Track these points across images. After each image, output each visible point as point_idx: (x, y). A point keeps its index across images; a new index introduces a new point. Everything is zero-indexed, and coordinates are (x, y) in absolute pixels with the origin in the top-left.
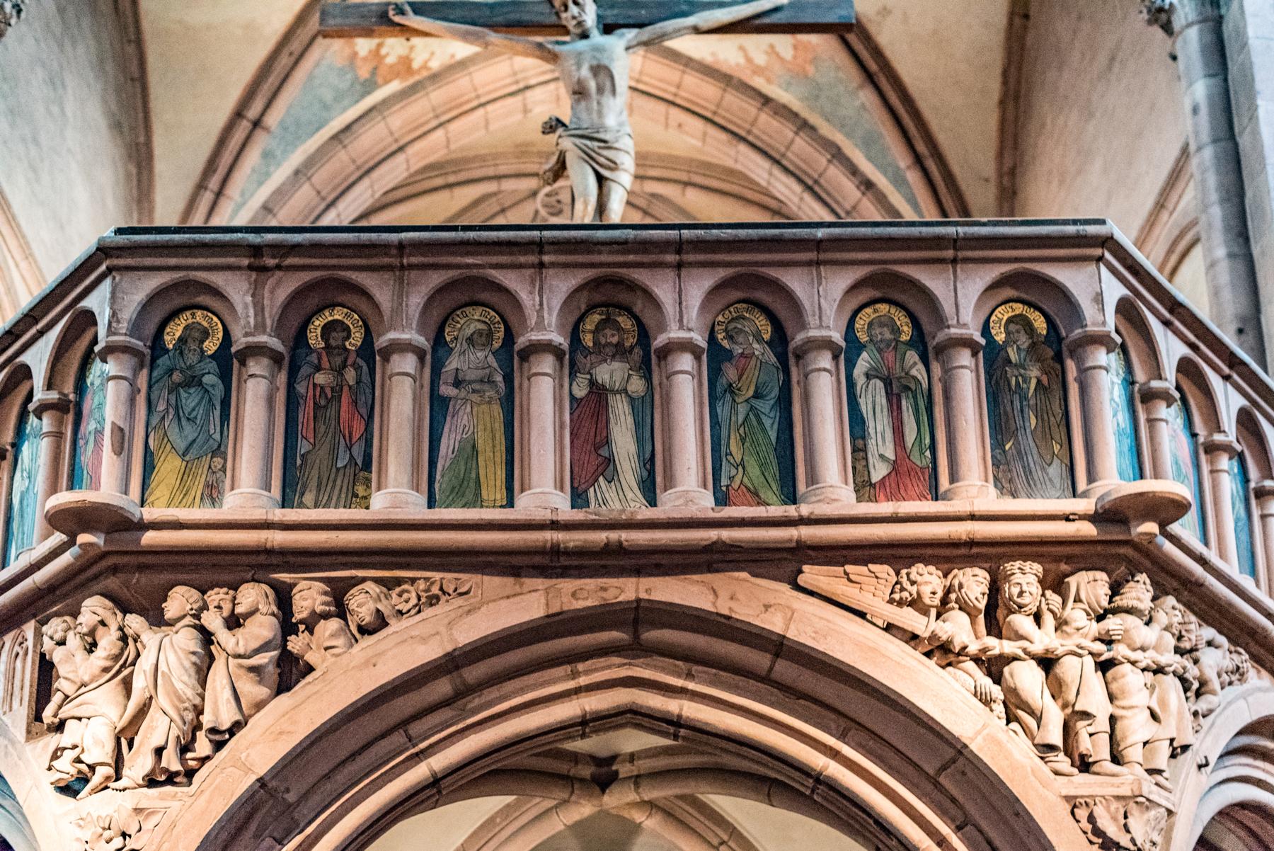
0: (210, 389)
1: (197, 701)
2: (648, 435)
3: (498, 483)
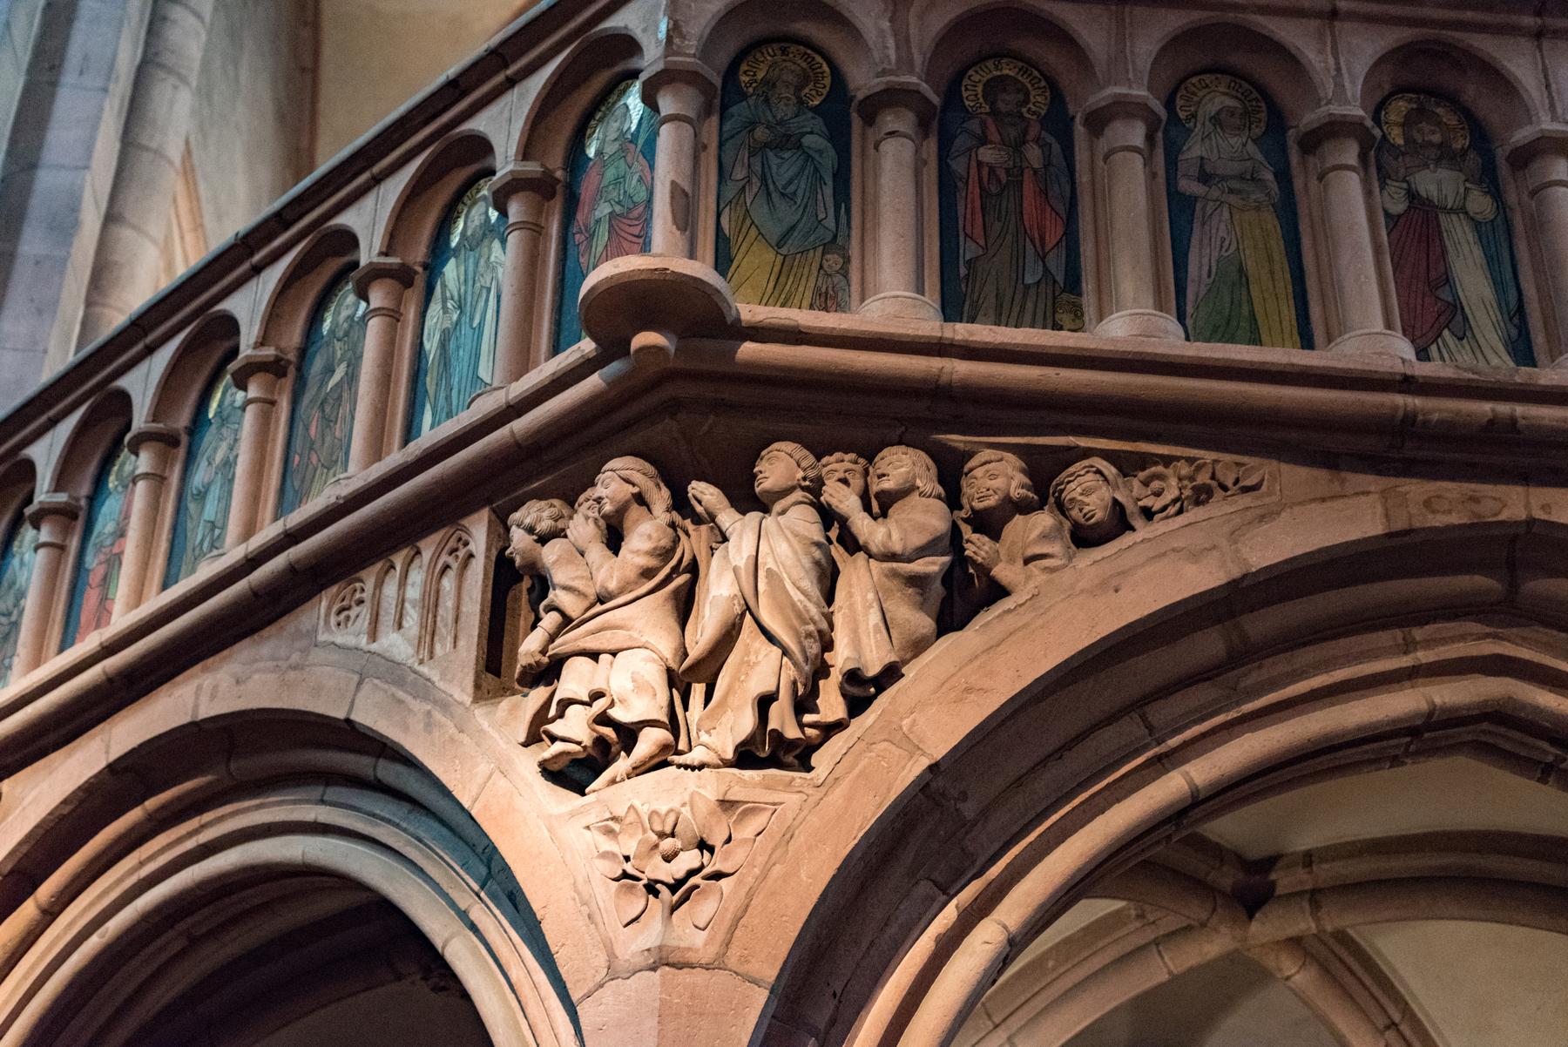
0: (817, 156)
1: (824, 626)
2: (1508, 275)
3: (1286, 324)
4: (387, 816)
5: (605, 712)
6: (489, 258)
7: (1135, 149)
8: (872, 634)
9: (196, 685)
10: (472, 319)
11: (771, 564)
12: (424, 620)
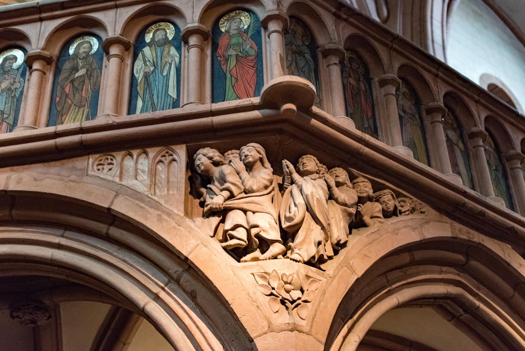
5: (258, 233)
6: (169, 52)
7: (393, 95)
8: (342, 229)
9: (6, 175)
10: (162, 72)
11: (318, 197)
12: (152, 179)
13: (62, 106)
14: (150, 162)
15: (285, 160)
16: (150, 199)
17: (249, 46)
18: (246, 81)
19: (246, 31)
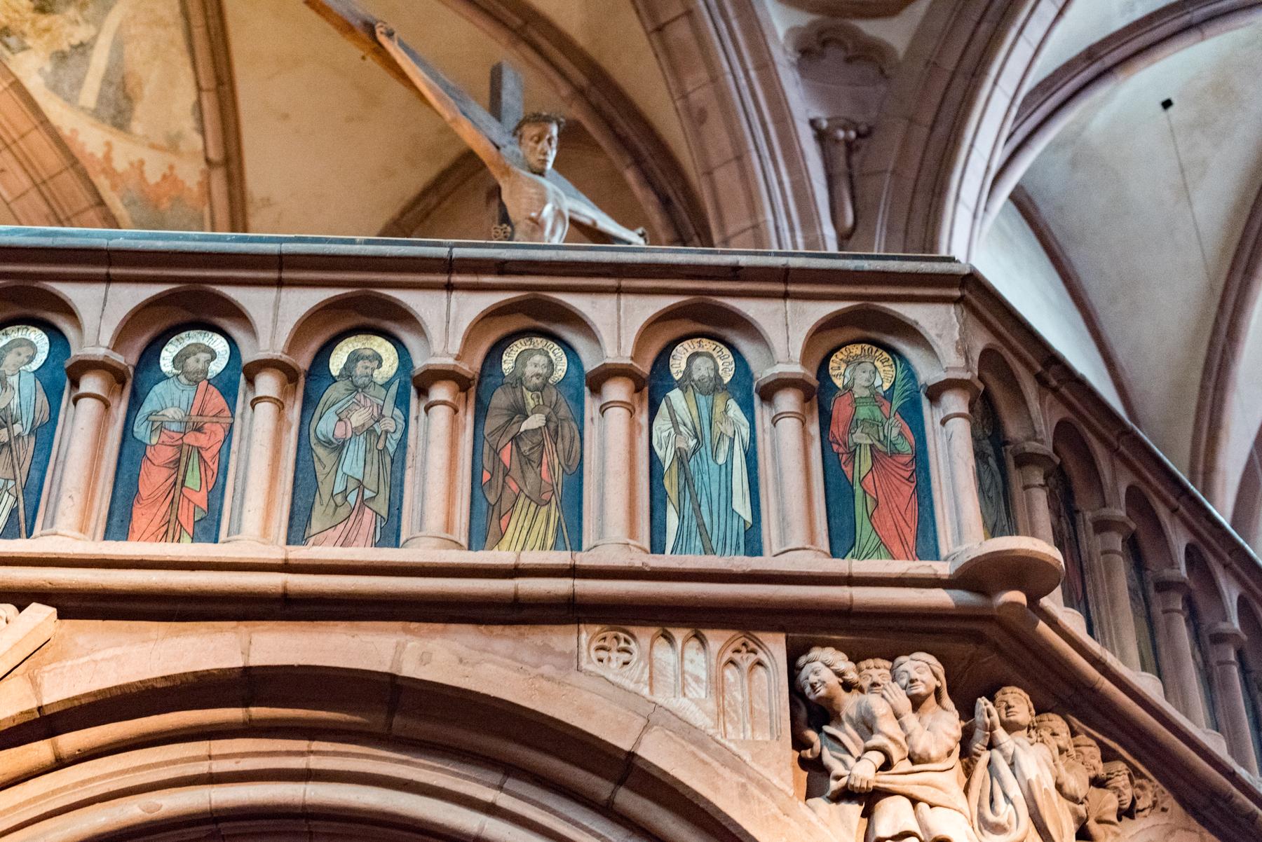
4: (599, 831)
6: (726, 411)
10: (715, 457)
13: (499, 494)
14: (714, 662)
15: (983, 697)
16: (719, 746)
17: (896, 429)
18: (896, 510)
19: (889, 395)
